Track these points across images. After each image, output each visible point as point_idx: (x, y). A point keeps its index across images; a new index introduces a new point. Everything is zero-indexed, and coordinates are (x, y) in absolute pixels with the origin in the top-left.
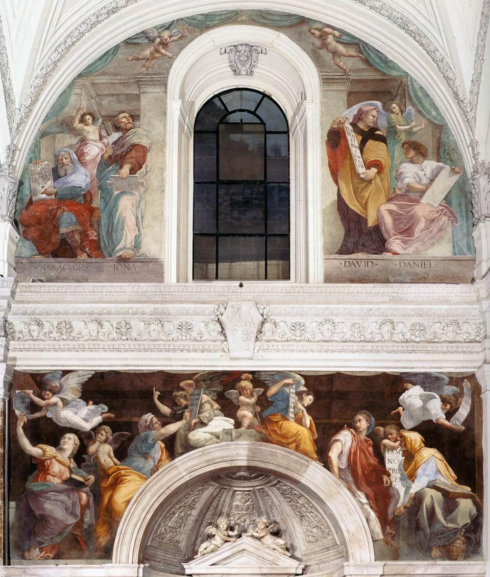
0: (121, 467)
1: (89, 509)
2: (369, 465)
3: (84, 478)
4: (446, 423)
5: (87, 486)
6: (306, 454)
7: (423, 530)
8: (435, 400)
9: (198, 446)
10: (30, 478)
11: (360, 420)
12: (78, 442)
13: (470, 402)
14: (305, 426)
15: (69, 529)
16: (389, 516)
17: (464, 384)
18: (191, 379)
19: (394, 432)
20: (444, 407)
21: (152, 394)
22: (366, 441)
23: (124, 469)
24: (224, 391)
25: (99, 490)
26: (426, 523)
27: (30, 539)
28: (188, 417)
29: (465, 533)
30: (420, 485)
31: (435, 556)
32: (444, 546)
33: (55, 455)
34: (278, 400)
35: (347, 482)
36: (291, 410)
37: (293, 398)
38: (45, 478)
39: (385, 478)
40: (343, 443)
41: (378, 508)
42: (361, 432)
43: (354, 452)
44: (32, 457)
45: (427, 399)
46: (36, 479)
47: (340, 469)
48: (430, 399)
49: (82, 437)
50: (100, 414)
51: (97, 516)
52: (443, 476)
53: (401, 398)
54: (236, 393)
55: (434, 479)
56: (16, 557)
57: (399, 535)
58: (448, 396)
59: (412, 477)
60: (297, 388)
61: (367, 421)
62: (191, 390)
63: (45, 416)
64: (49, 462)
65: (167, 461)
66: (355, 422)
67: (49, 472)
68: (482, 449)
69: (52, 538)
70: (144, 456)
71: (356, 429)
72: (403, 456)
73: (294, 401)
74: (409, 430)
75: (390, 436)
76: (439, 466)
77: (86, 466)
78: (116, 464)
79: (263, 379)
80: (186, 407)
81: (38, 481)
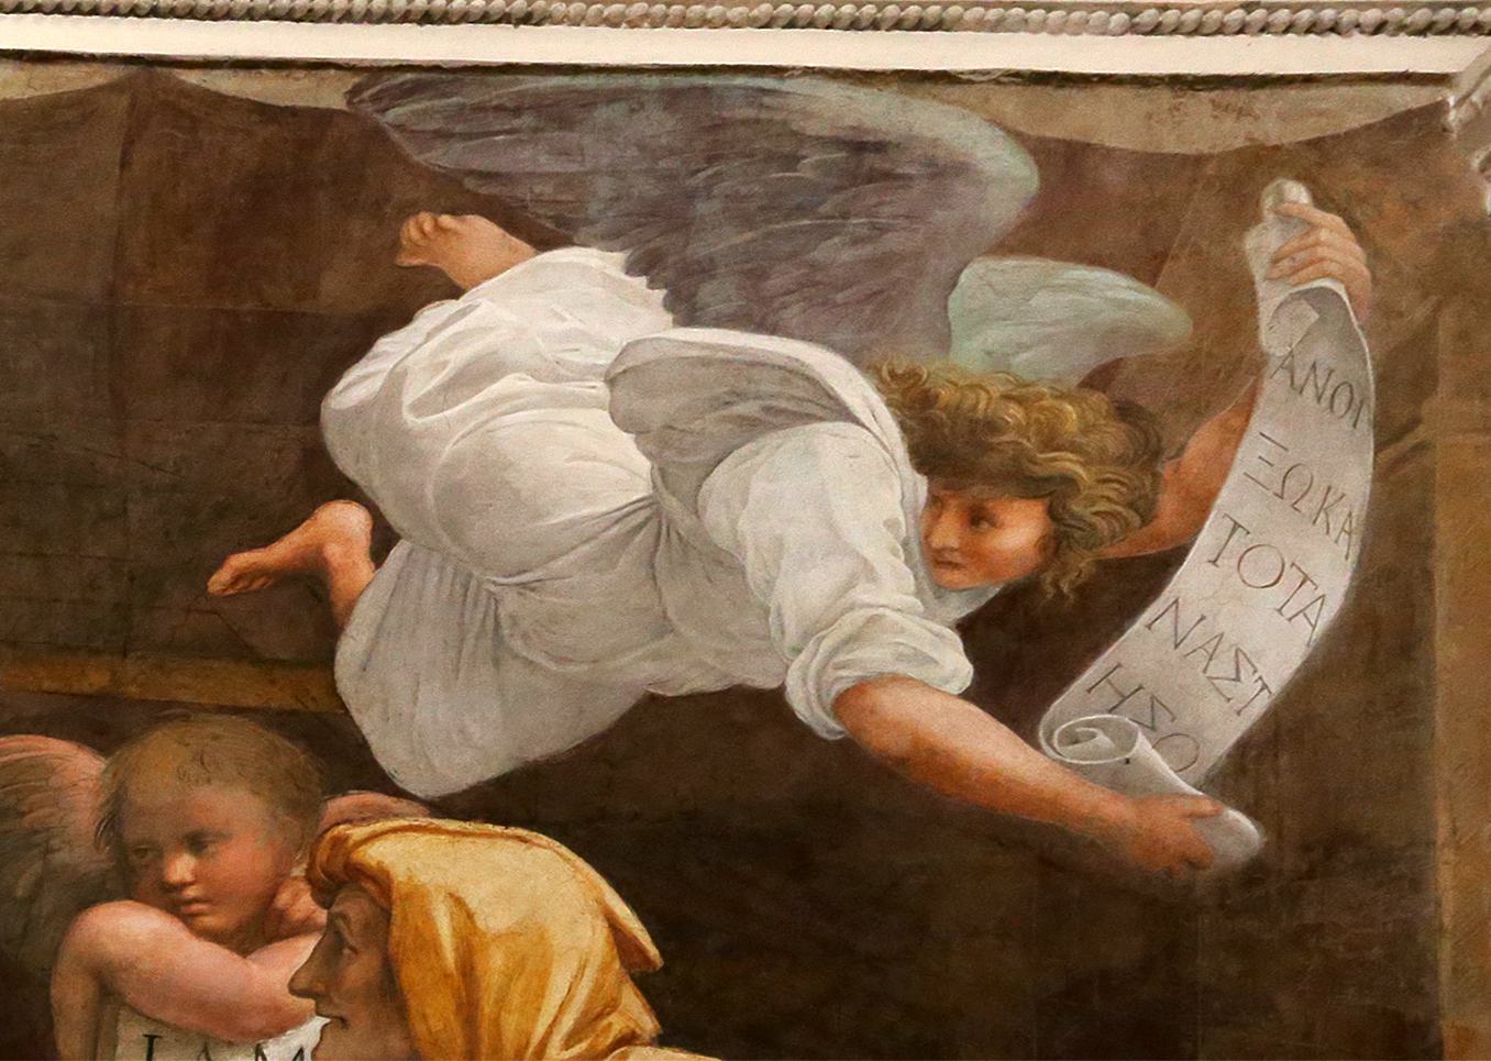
8: (827, 436)
17: (1262, 243)
20: (949, 533)
48: (752, 427)
53: (355, 388)
58: (1020, 396)
74: (444, 807)
75: (182, 867)
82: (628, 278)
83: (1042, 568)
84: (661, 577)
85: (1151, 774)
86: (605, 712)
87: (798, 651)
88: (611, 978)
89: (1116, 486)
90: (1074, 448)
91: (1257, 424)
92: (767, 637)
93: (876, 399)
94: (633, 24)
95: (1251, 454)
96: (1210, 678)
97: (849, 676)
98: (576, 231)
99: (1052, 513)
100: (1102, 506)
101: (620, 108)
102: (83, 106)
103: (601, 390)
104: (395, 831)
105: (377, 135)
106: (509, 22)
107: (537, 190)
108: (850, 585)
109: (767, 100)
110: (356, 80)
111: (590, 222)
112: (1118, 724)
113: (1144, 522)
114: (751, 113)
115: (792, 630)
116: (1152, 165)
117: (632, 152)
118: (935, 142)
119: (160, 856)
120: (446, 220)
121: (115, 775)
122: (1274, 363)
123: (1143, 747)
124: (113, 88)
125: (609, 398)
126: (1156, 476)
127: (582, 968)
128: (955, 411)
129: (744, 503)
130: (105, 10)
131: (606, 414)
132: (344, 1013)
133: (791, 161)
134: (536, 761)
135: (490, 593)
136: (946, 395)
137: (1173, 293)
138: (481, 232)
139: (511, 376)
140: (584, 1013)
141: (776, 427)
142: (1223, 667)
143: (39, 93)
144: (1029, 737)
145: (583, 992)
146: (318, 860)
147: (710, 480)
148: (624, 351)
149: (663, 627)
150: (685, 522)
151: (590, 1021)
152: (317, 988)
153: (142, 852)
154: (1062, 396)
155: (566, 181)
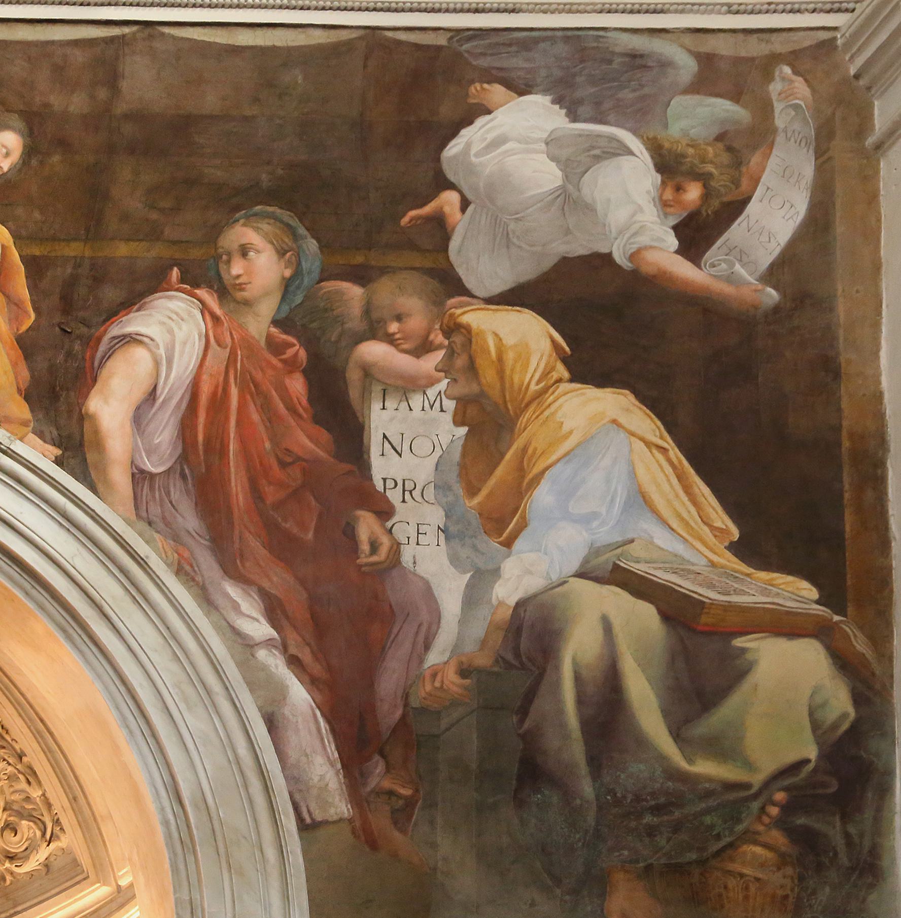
11: (244, 251)
13: (808, 171)
16: (383, 708)
17: (775, 88)
20: (669, 195)
22: (276, 348)
26: (577, 751)
40: (162, 351)
41: (329, 669)
42: (247, 303)
43: (214, 394)
47: (139, 476)
48: (598, 159)
53: (453, 149)
61: (281, 253)
66: (218, 258)
68: (879, 397)
71: (223, 292)
74: (490, 301)
75: (393, 327)
76: (641, 471)
82: (552, 106)
83: (702, 206)
84: (567, 214)
87: (616, 239)
88: (553, 359)
89: (726, 176)
90: (711, 162)
91: (775, 152)
92: (605, 234)
94: (552, 12)
95: (773, 163)
96: (760, 242)
97: (635, 247)
98: (533, 88)
99: (705, 186)
100: (722, 183)
101: (549, 43)
102: (349, 45)
103: (543, 146)
104: (472, 310)
105: (459, 55)
106: (507, 12)
107: (519, 74)
108: (633, 215)
109: (601, 40)
110: (451, 34)
111: (537, 85)
112: (729, 260)
113: (737, 188)
114: (595, 44)
115: (613, 230)
116: (737, 61)
117: (553, 59)
118: (661, 54)
120: (486, 86)
121: (368, 295)
122: (780, 130)
123: (738, 267)
124: (359, 38)
125: (546, 149)
126: (740, 171)
127: (542, 356)
128: (670, 151)
129: (596, 187)
130: (356, 9)
131: (545, 156)
132: (455, 377)
133: (610, 62)
134: (523, 283)
135: (505, 222)
136: (667, 145)
137: (744, 106)
138: (497, 91)
139: (510, 143)
140: (543, 373)
141: (606, 159)
142: (764, 238)
143: (332, 40)
144: (699, 266)
146: (444, 321)
147: (583, 179)
148: (552, 132)
149: (568, 232)
150: (575, 194)
151: (545, 375)
152: (445, 369)
153: (378, 322)
154: (708, 144)
155: (529, 71)
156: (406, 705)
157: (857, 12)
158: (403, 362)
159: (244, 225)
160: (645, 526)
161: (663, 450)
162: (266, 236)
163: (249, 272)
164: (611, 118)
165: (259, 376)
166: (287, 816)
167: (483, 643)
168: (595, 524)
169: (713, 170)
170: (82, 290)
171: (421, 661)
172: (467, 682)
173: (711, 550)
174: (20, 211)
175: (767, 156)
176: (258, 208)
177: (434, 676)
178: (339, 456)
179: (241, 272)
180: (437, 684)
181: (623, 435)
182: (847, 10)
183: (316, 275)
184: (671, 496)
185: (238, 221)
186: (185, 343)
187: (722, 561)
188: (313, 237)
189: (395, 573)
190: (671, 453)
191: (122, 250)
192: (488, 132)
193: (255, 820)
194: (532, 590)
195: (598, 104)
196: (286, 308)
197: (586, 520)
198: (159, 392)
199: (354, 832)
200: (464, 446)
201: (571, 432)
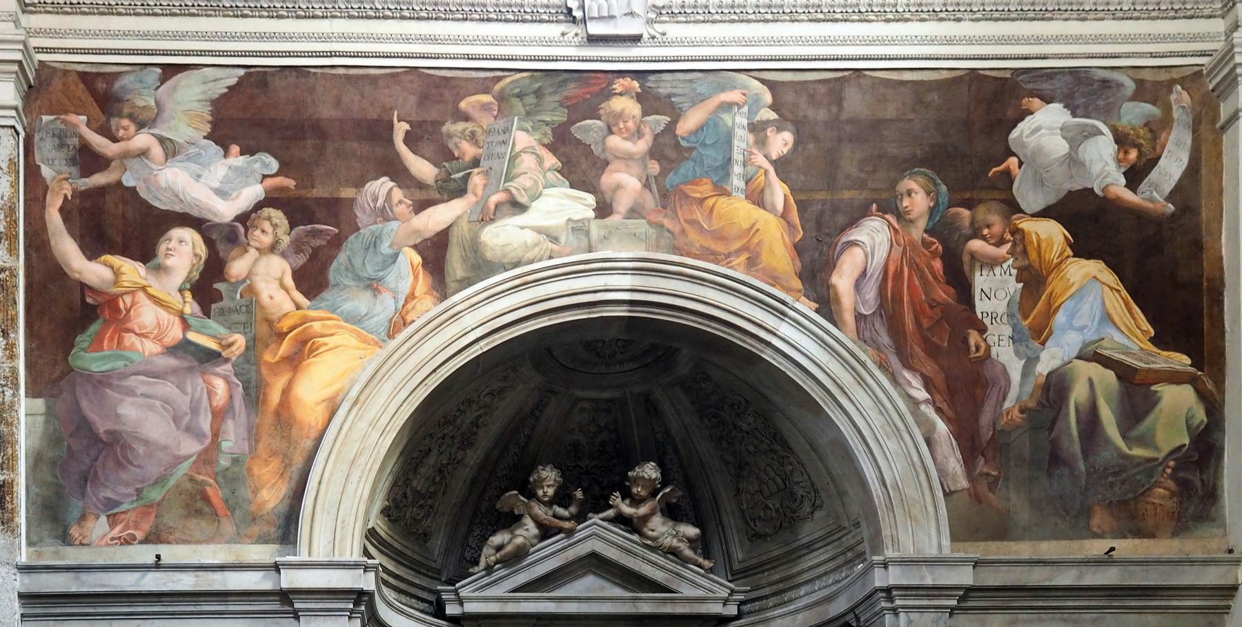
0: (312, 313)
1: (234, 418)
2: (933, 304)
3: (219, 339)
4: (1128, 195)
5: (227, 360)
6: (775, 280)
7: (1069, 464)
8: (1100, 138)
9: (505, 261)
10: (83, 340)
11: (909, 193)
12: (202, 250)
14: (773, 210)
15: (184, 468)
16: (984, 431)
17: (1173, 97)
18: (486, 91)
19: (995, 221)
20: (1121, 156)
21: (391, 127)
22: (926, 245)
23: (319, 318)
24: (571, 122)
25: (258, 372)
27: (83, 495)
28: (481, 187)
29: (1175, 470)
30: (1061, 355)
31: (1099, 527)
32: (1124, 503)
33: (144, 283)
34: (706, 145)
35: (878, 348)
36: (737, 169)
37: (741, 139)
38: (120, 342)
39: (974, 337)
41: (956, 413)
42: (911, 221)
43: (896, 271)
44: (84, 287)
45: (1079, 137)
46: (97, 345)
47: (859, 317)
48: (1086, 137)
49: (214, 237)
50: (259, 178)
51: (253, 435)
52: (1118, 328)
54: (600, 127)
55: (1096, 338)
56: (49, 540)
57: (1007, 479)
59: (1041, 332)
60: (752, 113)
61: (928, 194)
62: (486, 120)
63: (119, 183)
64: (128, 299)
65: (428, 301)
67: (129, 325)
69: (139, 491)
70: (369, 287)
71: (900, 215)
72: (1018, 281)
73: (744, 146)
74: (1033, 216)
75: (986, 231)
76: (1107, 303)
77: (222, 312)
78: (298, 307)
79: (669, 91)
80: (476, 163)
81: (101, 349)
83: (1137, 162)
85: (1156, 198)
86: (1062, 194)
93: (1108, 131)
95: (1172, 137)
97: (1105, 184)
99: (1139, 151)
116: (1155, 83)
119: (981, 229)
123: (1155, 193)
131: (1060, 137)
136: (1120, 129)
144: (1136, 193)
145: (1060, 248)
149: (1072, 177)
152: (1012, 252)
154: (1140, 128)
156: (994, 430)
157: (1214, 57)
158: (990, 250)
159: (909, 179)
160: (1110, 331)
161: (1118, 291)
162: (920, 185)
163: (912, 204)
164: (1093, 115)
165: (918, 260)
166: (938, 491)
167: (1032, 395)
168: (1085, 331)
169: (1143, 142)
170: (827, 217)
171: (1001, 407)
172: (1024, 415)
173: (1142, 342)
174: (793, 176)
175: (1169, 135)
176: (916, 169)
177: (1008, 413)
178: (959, 301)
179: (908, 204)
180: (1009, 417)
181: (1099, 284)
182: (1208, 55)
183: (946, 205)
184: (1122, 315)
185: (905, 177)
186: (880, 244)
187: (1146, 347)
188: (945, 184)
189: (988, 361)
190: (1122, 293)
191: (847, 195)
192: (1032, 124)
193: (923, 493)
194: (1055, 367)
195: (1086, 108)
196: (932, 223)
197: (1081, 329)
198: (867, 271)
199: (970, 495)
200: (1022, 293)
201: (1074, 283)
